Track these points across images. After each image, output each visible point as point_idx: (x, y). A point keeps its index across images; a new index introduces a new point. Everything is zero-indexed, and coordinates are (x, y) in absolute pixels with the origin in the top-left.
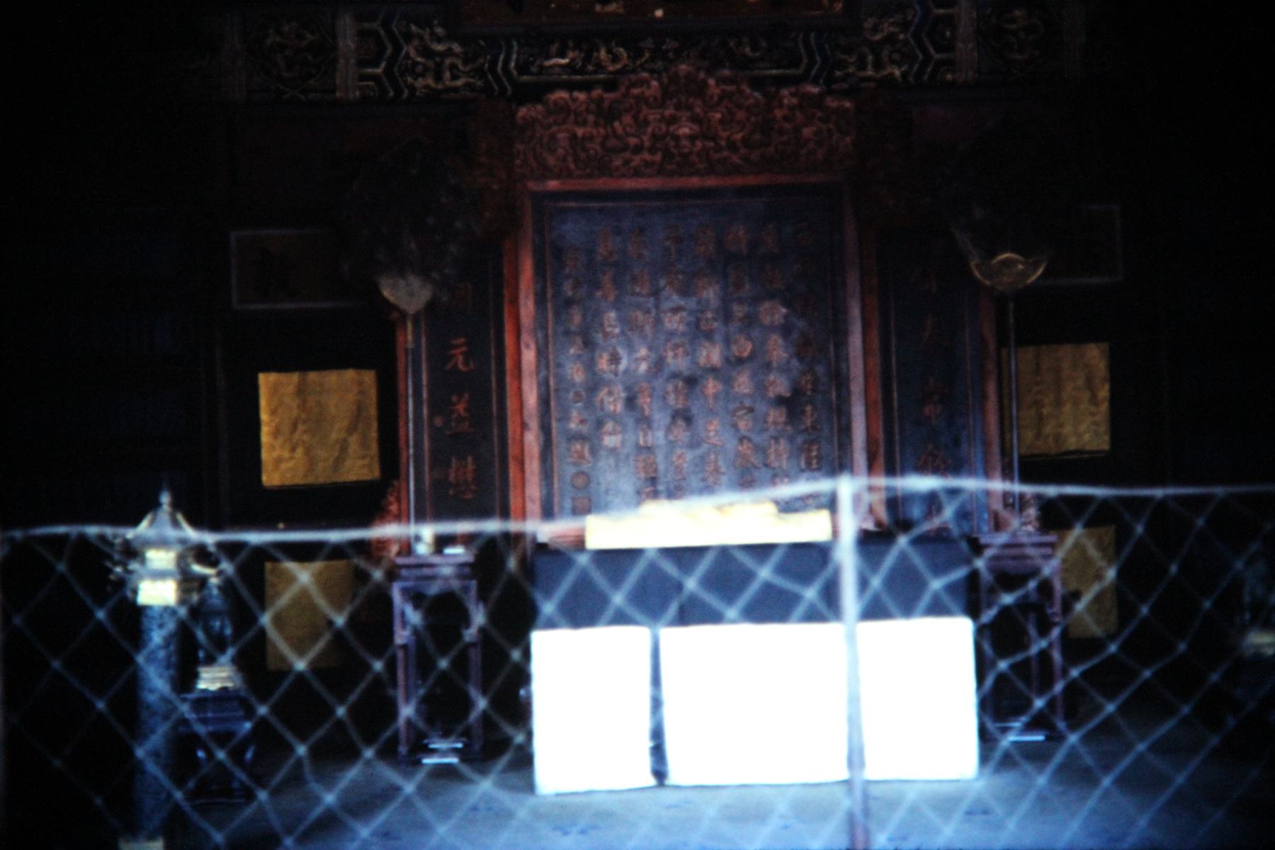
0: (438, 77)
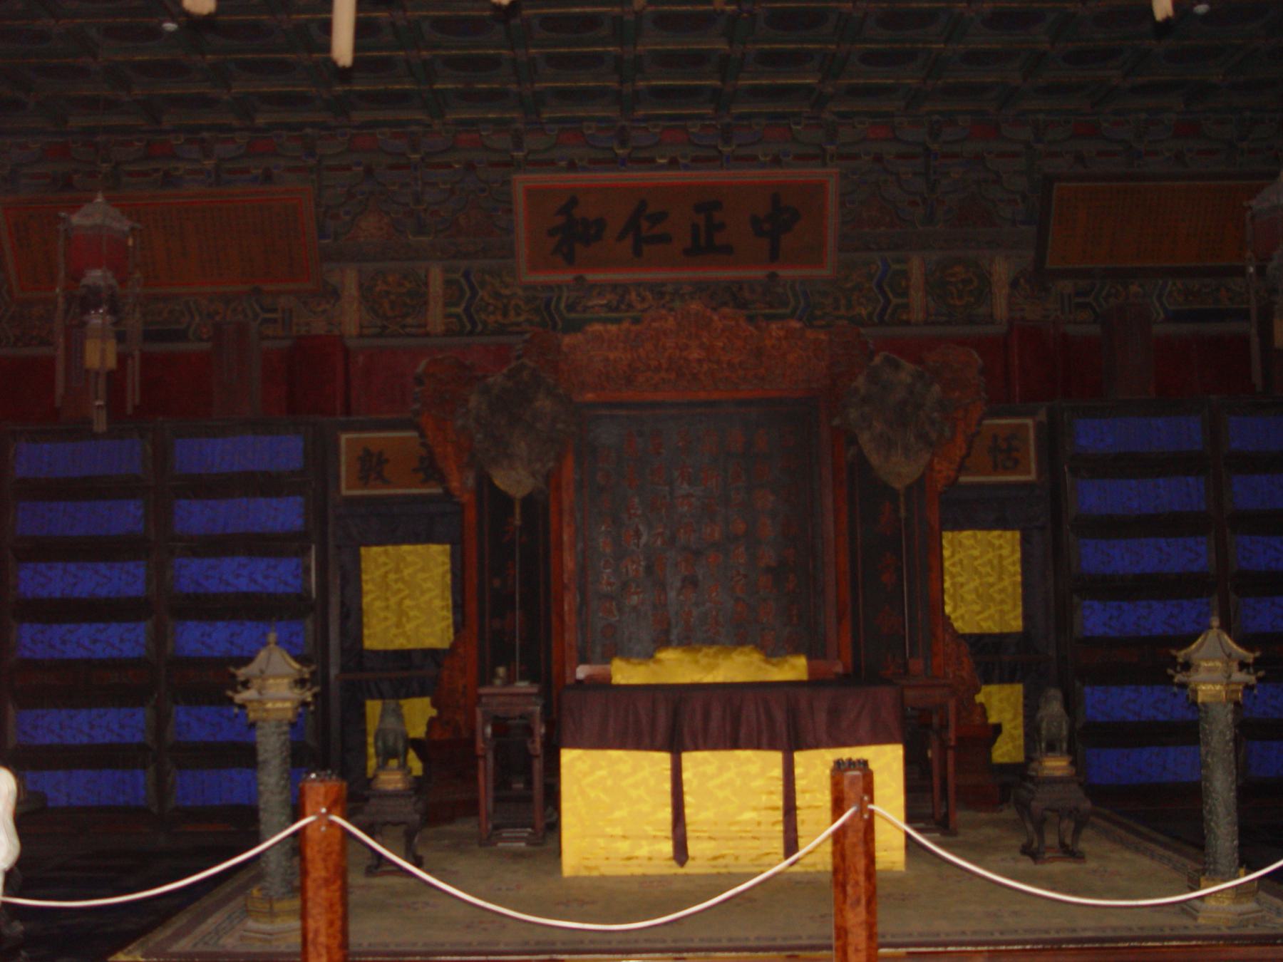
0: (505, 315)
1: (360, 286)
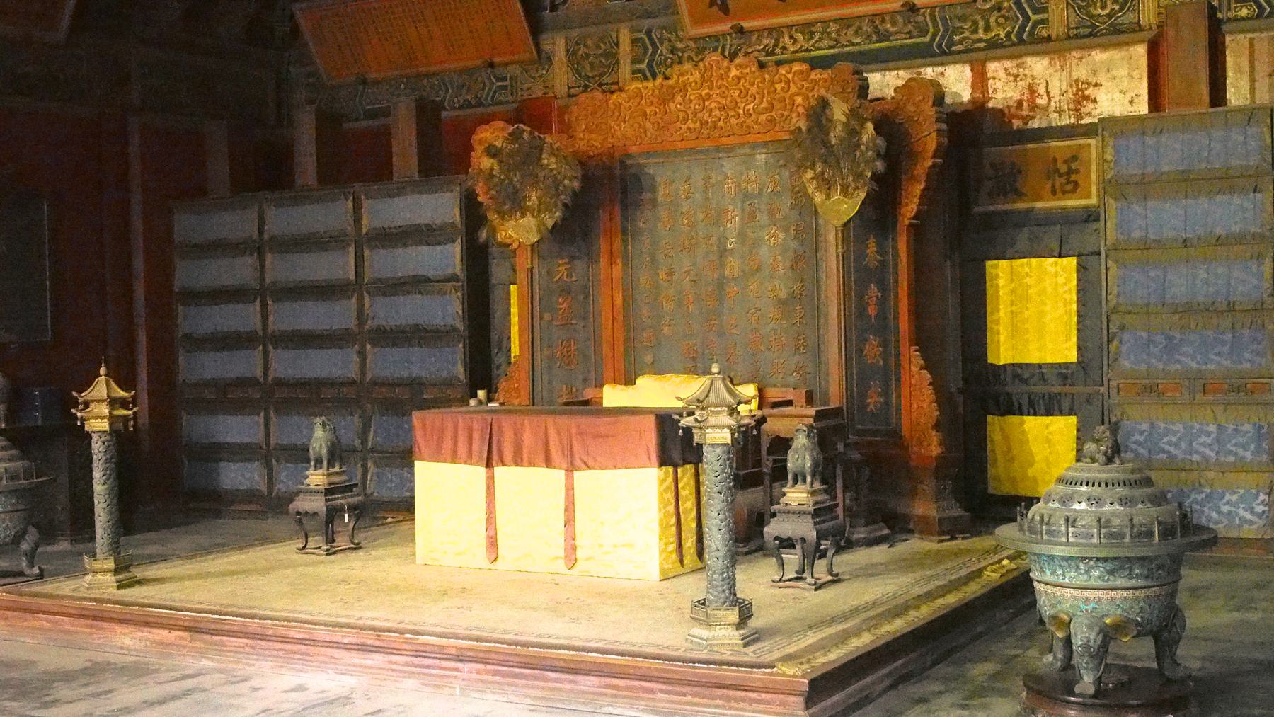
1: (568, 51)
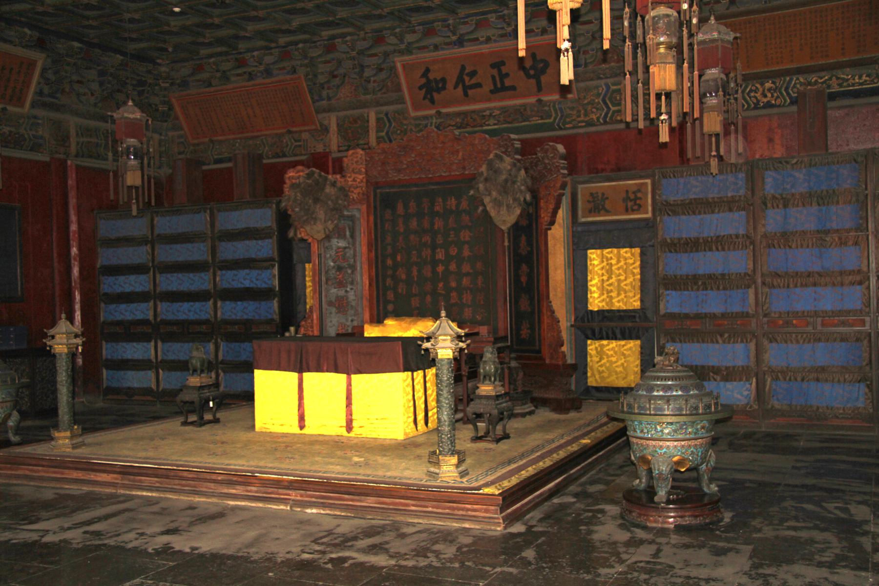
1: (338, 124)
